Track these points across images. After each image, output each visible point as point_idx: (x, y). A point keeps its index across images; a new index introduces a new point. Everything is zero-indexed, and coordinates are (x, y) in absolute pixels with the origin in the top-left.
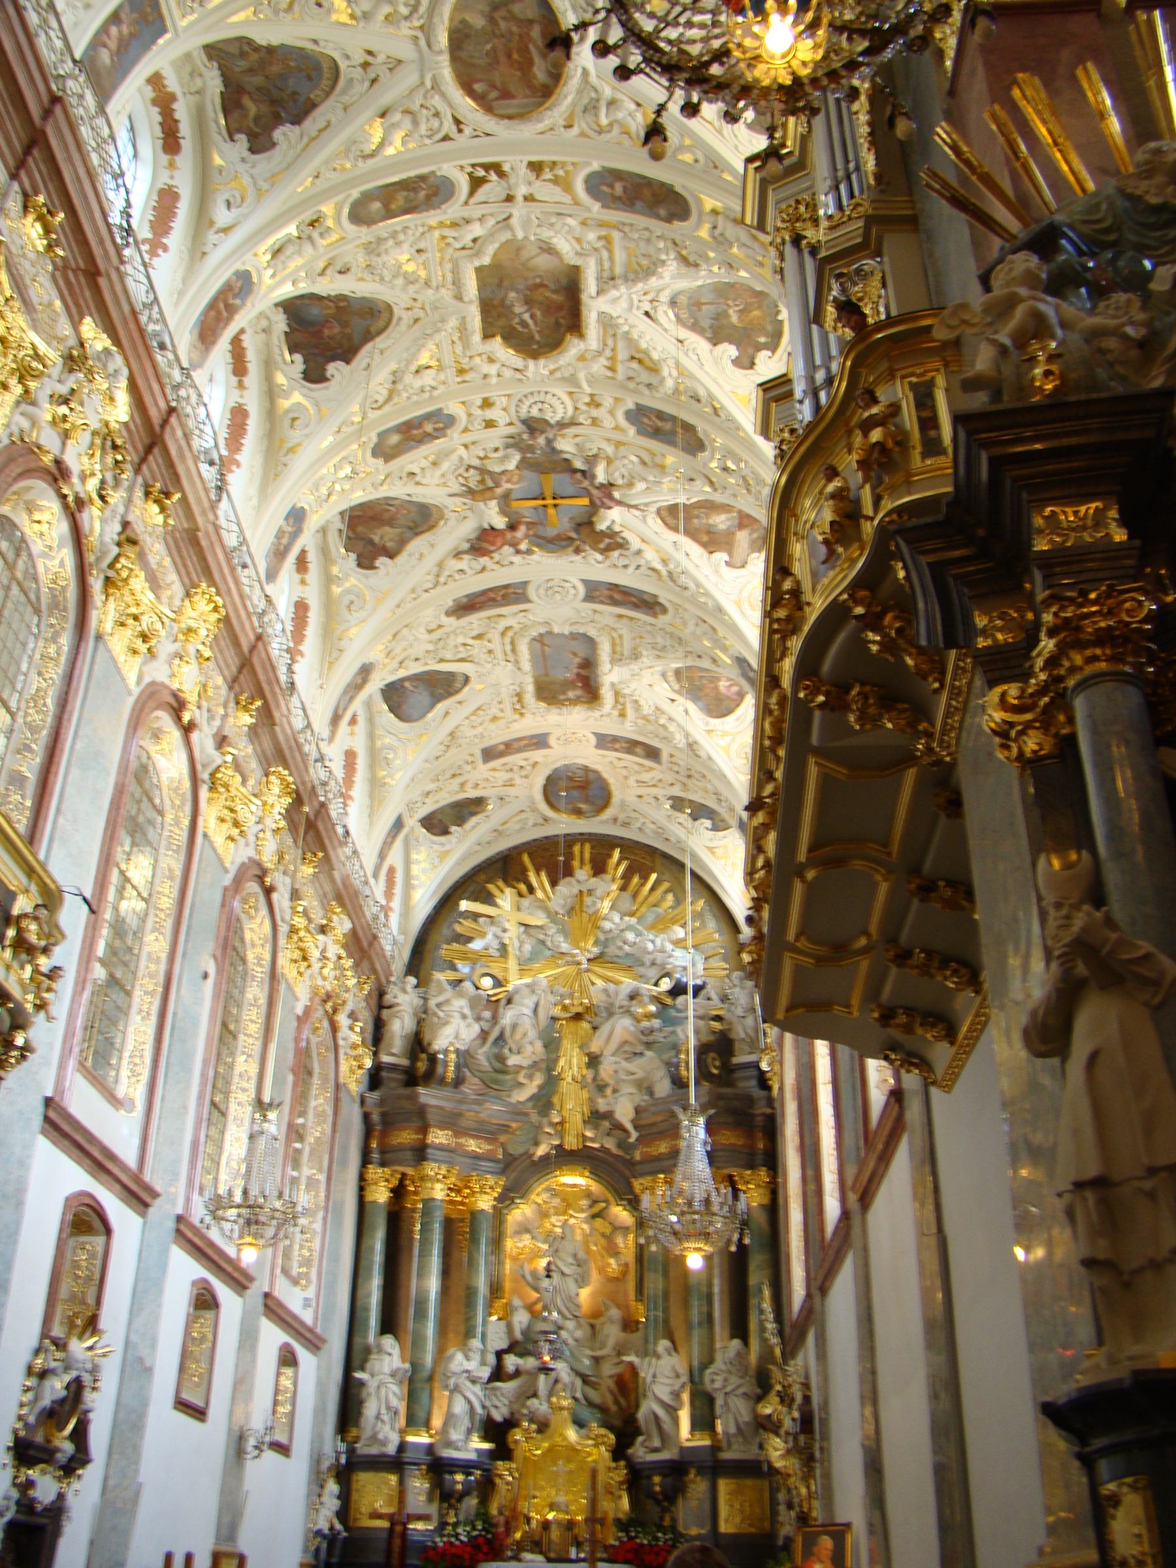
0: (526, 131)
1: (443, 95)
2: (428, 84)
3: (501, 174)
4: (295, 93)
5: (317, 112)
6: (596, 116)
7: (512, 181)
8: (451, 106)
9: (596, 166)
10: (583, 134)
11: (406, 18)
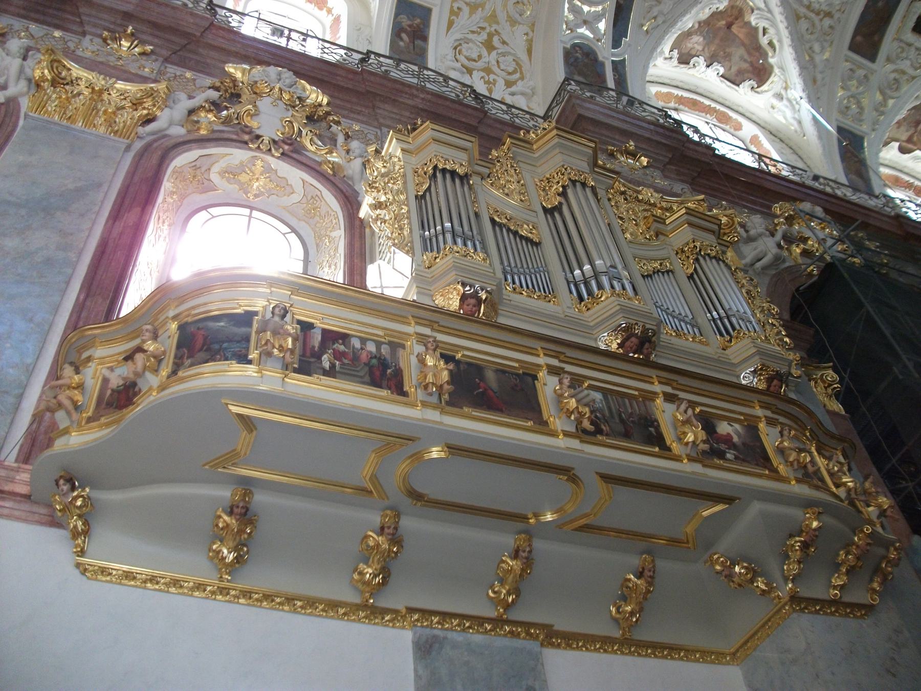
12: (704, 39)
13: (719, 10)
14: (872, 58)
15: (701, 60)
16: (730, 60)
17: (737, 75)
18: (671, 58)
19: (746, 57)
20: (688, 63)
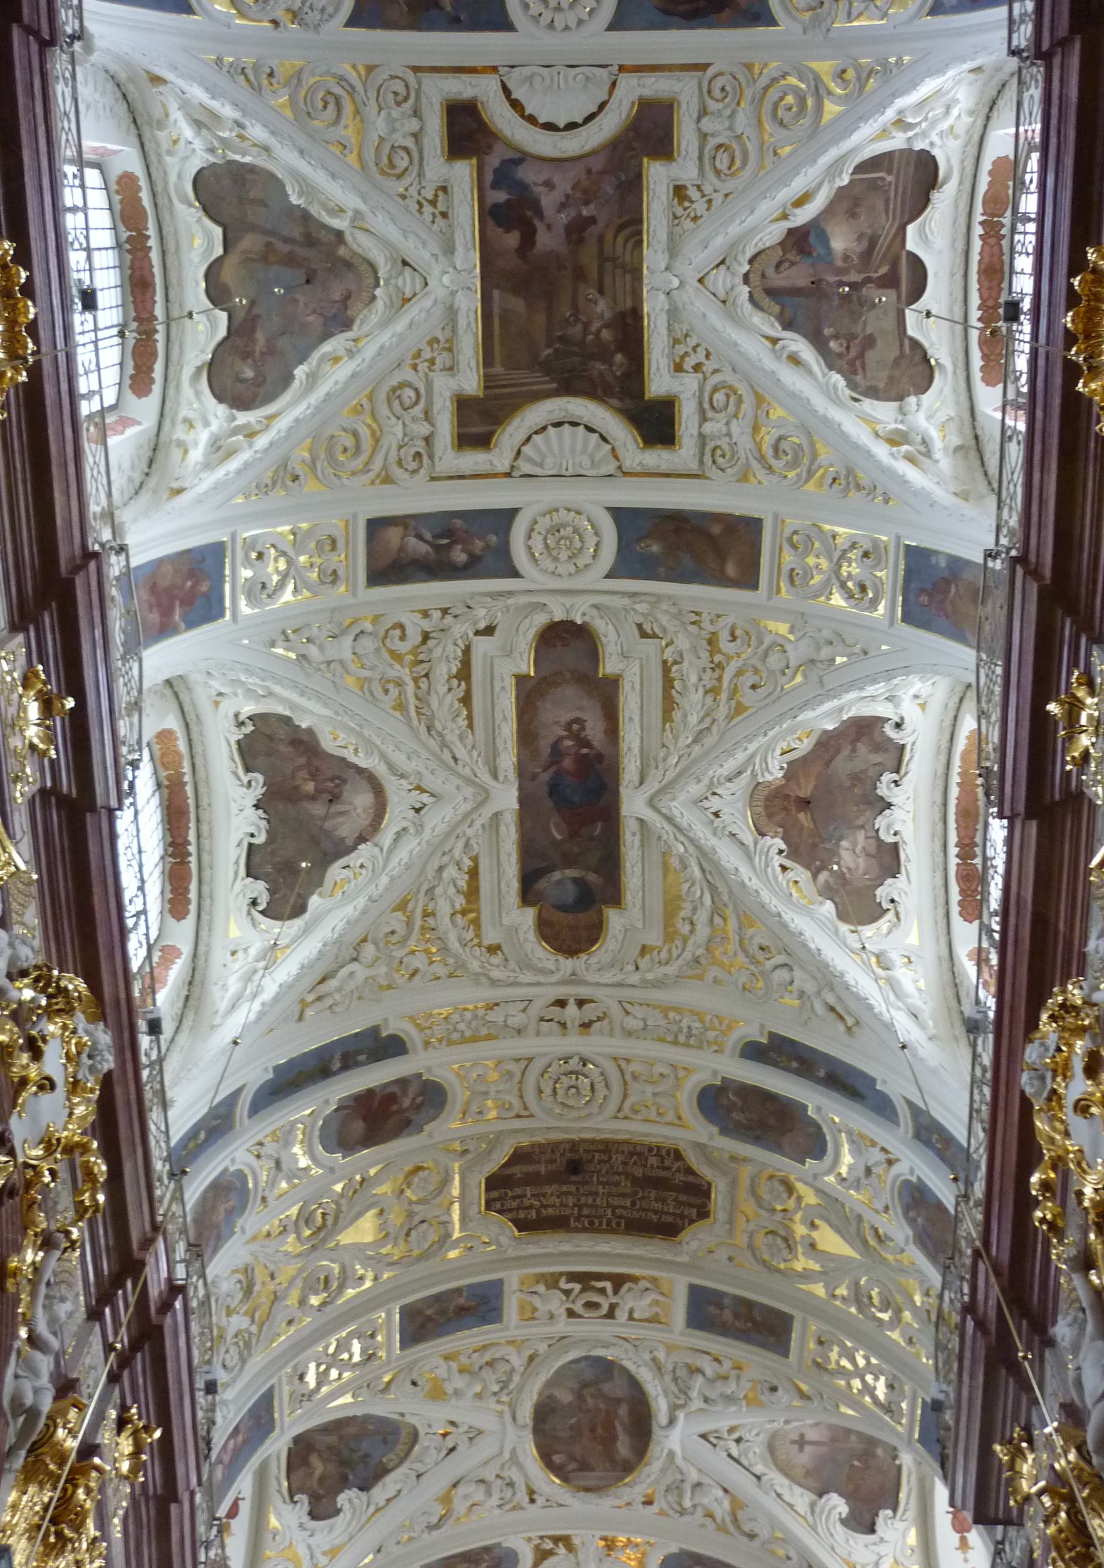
0: (602, 1506)
1: (520, 1467)
2: (507, 1455)
3: (570, 1548)
4: (366, 1456)
5: (389, 1479)
6: (681, 1496)
7: (581, 1557)
8: (526, 1476)
9: (674, 1549)
10: (662, 1513)
11: (495, 1394)
12: (841, 838)
13: (783, 847)
14: (754, 525)
15: (880, 822)
16: (865, 771)
17: (886, 750)
18: (892, 901)
19: (846, 752)
20: (895, 846)
